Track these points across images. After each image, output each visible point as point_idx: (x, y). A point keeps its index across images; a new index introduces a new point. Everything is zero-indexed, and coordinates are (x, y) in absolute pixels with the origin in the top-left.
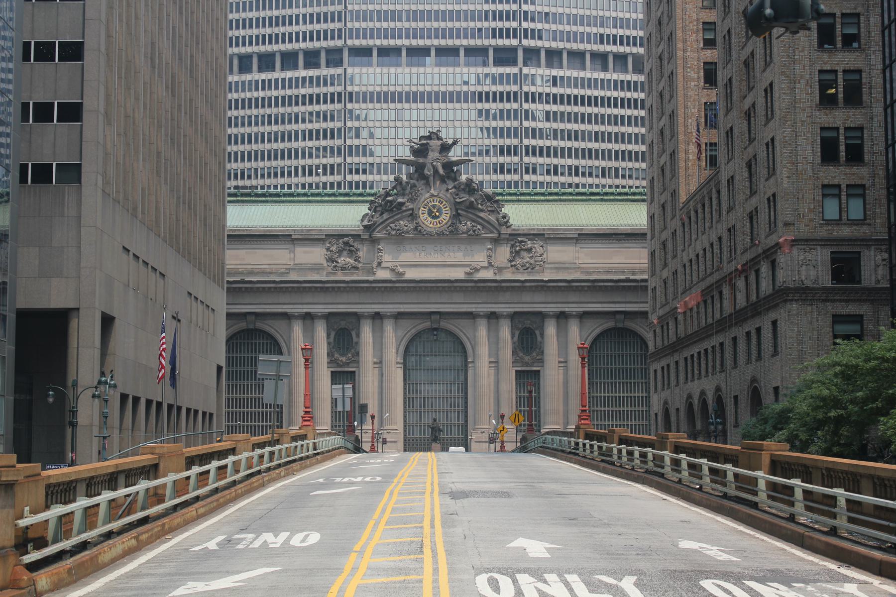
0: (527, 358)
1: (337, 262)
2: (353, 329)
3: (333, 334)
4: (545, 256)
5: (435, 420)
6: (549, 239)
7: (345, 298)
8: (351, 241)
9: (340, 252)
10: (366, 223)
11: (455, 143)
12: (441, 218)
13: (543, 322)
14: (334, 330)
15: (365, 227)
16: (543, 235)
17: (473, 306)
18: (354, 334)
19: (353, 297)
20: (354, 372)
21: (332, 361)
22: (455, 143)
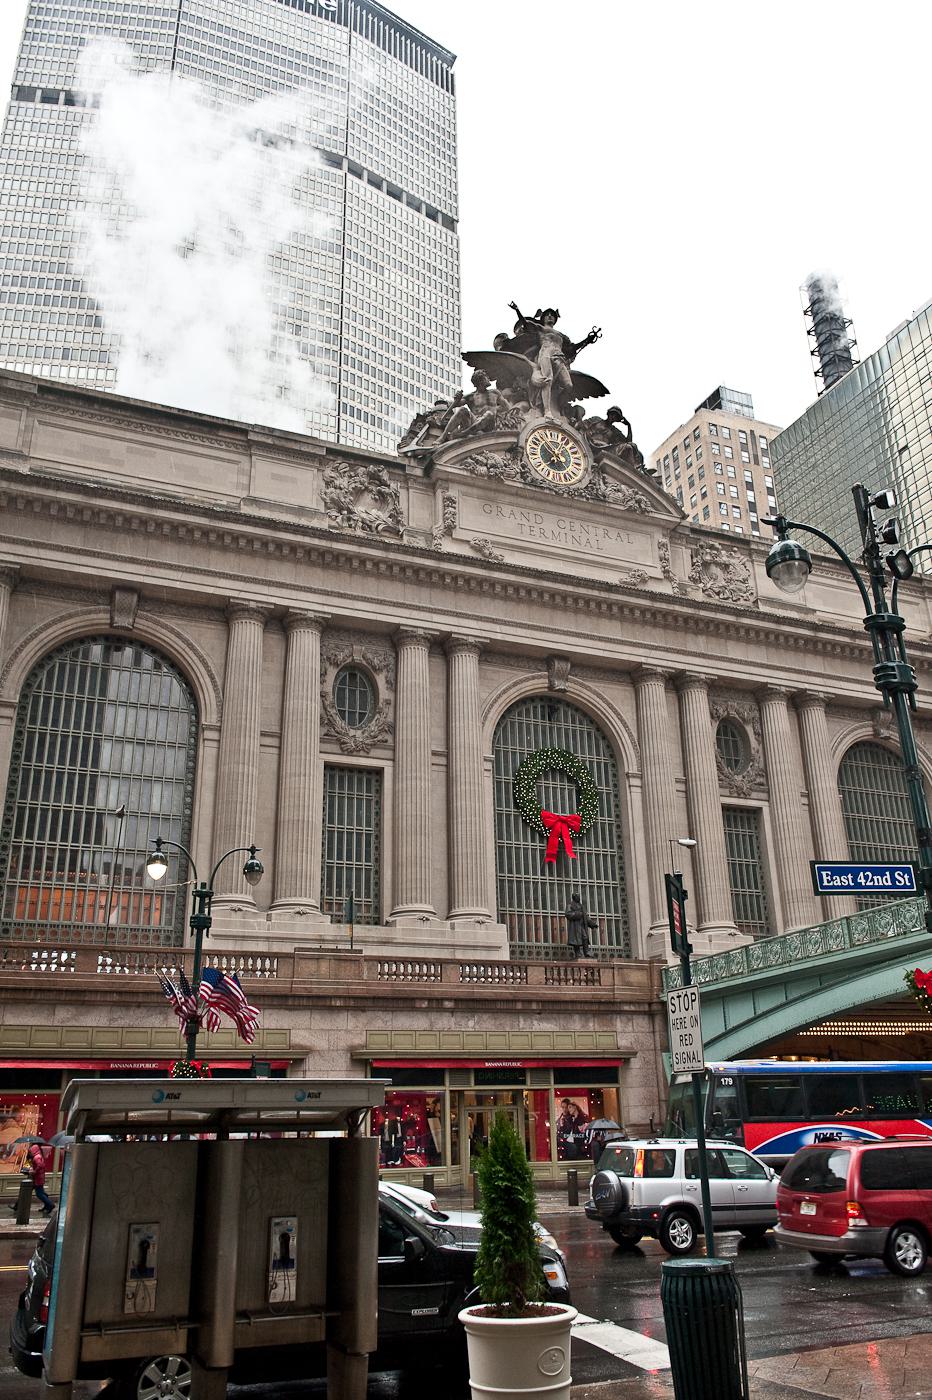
0: (740, 778)
1: (350, 512)
2: (378, 670)
3: (332, 672)
4: (751, 583)
5: (576, 899)
7: (371, 587)
8: (385, 476)
9: (358, 492)
10: (413, 446)
11: (590, 339)
12: (571, 468)
13: (760, 710)
14: (336, 665)
15: (415, 455)
16: (747, 543)
17: (641, 651)
18: (381, 680)
19: (393, 591)
20: (379, 772)
21: (330, 736)
22: (590, 339)
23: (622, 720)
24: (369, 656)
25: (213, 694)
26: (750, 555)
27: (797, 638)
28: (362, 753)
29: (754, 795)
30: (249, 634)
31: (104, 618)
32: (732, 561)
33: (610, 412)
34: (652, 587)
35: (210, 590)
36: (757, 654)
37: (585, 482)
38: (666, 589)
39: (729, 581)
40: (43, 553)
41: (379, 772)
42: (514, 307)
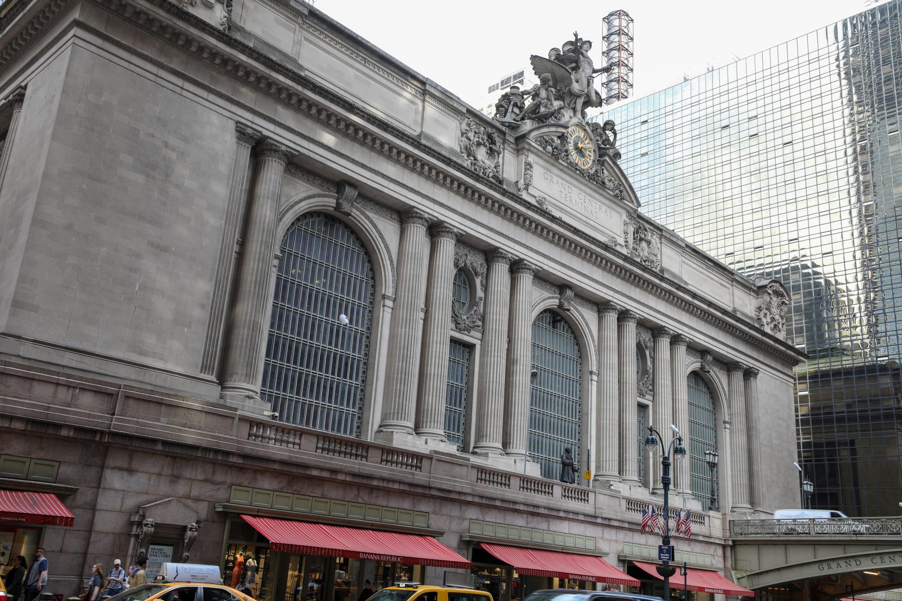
1: (475, 159)
6: (666, 237)
9: (479, 144)
16: (661, 230)
17: (611, 293)
18: (478, 281)
20: (470, 347)
21: (455, 318)
23: (592, 336)
24: (475, 264)
25: (390, 274)
26: (660, 239)
27: (683, 300)
28: (466, 332)
29: (647, 397)
30: (418, 234)
31: (332, 202)
32: (653, 241)
33: (606, 124)
34: (618, 248)
35: (403, 199)
36: (661, 306)
37: (594, 170)
38: (624, 251)
39: (649, 253)
40: (312, 147)
41: (474, 345)
42: (576, 35)
